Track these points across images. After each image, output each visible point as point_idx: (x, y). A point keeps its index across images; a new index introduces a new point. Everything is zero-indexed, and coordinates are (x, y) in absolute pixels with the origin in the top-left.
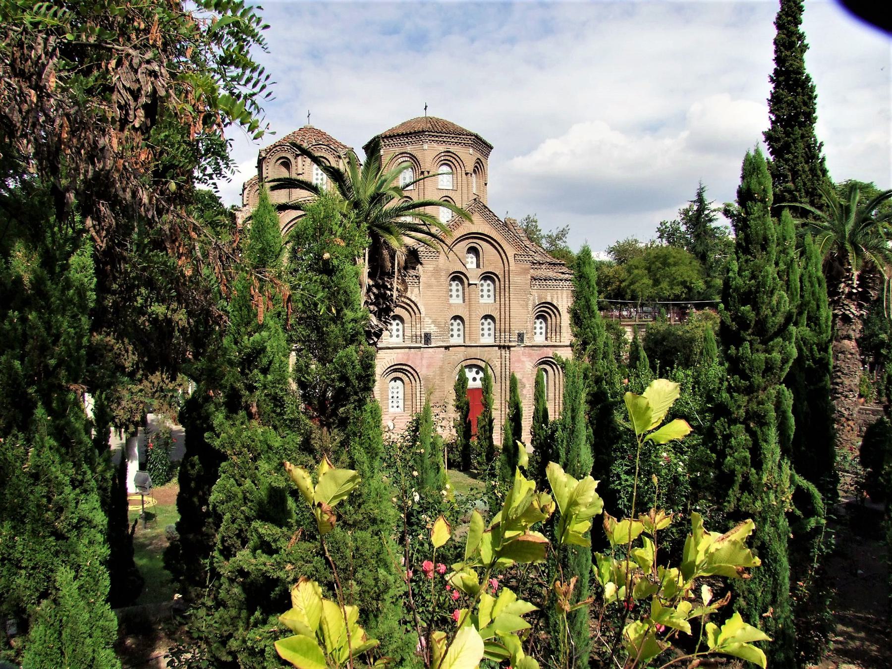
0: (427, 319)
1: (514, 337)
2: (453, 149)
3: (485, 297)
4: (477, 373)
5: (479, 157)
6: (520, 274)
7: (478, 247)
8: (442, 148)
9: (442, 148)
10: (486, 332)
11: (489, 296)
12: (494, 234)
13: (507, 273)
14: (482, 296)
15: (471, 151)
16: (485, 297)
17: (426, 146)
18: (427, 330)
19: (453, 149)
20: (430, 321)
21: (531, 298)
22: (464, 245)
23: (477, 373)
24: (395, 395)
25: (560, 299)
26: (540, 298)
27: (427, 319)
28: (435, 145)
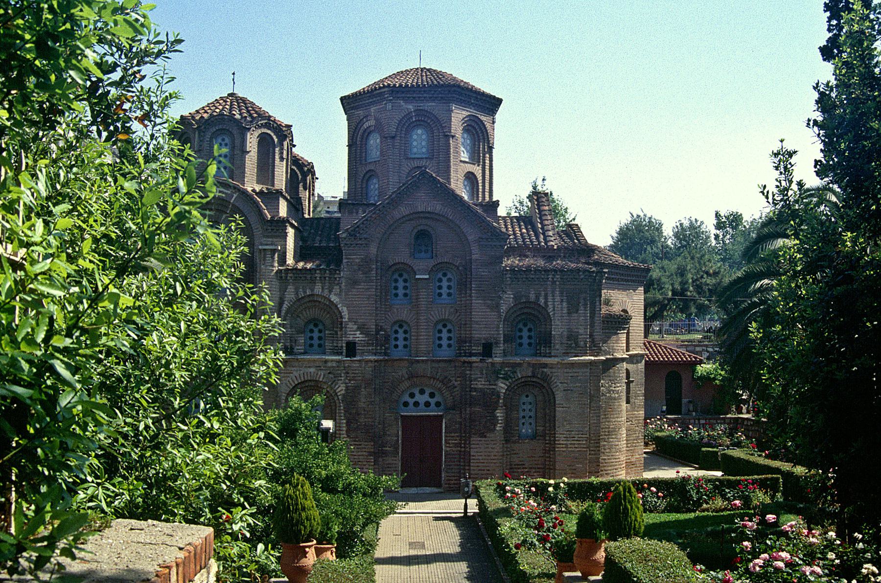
0: (350, 325)
8: (411, 107)
11: (449, 295)
14: (440, 295)
23: (432, 395)
25: (550, 298)
27: (350, 325)
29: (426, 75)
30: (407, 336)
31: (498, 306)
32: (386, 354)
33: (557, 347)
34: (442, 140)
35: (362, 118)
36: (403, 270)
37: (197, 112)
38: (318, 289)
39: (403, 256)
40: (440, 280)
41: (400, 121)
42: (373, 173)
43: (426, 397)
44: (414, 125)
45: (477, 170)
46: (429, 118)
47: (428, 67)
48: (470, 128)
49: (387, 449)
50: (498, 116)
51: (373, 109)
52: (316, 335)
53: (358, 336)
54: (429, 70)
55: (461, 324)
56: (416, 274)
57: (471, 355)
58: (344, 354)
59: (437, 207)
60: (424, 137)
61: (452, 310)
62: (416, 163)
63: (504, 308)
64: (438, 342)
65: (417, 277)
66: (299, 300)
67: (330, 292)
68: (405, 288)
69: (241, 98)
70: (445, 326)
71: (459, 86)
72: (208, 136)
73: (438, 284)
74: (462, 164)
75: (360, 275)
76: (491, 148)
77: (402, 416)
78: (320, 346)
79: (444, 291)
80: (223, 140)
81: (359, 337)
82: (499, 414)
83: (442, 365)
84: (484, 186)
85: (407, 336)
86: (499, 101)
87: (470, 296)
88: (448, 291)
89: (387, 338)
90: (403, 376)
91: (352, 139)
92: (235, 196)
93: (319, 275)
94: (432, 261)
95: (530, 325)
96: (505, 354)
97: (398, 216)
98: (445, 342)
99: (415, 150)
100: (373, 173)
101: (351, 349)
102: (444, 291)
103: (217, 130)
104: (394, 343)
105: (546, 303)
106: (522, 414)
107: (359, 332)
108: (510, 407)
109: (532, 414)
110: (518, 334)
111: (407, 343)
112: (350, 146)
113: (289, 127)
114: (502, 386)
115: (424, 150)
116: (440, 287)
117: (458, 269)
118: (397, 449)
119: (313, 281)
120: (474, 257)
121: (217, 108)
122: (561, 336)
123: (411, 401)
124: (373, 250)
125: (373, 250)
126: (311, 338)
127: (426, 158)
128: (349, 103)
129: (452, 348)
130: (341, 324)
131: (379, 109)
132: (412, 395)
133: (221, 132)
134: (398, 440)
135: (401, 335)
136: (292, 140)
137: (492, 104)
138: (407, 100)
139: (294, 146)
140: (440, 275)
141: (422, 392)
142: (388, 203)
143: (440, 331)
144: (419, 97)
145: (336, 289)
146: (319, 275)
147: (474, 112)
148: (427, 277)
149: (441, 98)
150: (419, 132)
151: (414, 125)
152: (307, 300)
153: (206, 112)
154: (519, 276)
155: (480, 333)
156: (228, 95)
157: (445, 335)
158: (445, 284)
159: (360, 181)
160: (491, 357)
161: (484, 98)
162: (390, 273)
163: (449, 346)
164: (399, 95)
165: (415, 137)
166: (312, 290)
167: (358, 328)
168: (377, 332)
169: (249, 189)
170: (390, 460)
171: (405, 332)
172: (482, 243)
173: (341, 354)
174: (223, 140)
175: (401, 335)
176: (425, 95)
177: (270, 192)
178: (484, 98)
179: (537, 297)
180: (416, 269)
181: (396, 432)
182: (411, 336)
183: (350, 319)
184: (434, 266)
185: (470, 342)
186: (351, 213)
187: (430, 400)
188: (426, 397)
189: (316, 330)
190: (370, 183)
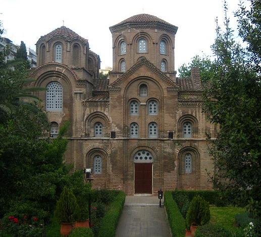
0: (113, 124)
2: (145, 30)
3: (153, 112)
4: (148, 154)
5: (165, 33)
6: (170, 99)
7: (145, 83)
8: (138, 31)
9: (138, 31)
10: (153, 132)
11: (155, 112)
12: (154, 76)
14: (151, 112)
15: (156, 31)
16: (153, 112)
18: (113, 130)
19: (145, 30)
23: (148, 154)
24: (98, 165)
25: (197, 113)
27: (113, 124)
31: (175, 116)
32: (128, 137)
33: (201, 134)
36: (134, 101)
38: (99, 110)
39: (135, 95)
40: (151, 105)
51: (123, 32)
52: (99, 129)
57: (166, 137)
59: (149, 74)
60: (144, 44)
63: (178, 118)
66: (91, 114)
67: (104, 110)
71: (159, 22)
72: (52, 45)
76: (174, 48)
77: (135, 163)
78: (100, 133)
81: (116, 129)
82: (176, 163)
83: (152, 141)
89: (128, 130)
95: (189, 125)
96: (178, 136)
98: (153, 132)
99: (141, 49)
101: (113, 135)
102: (153, 110)
104: (132, 132)
105: (196, 115)
106: (186, 163)
108: (180, 160)
109: (191, 163)
110: (184, 128)
112: (113, 48)
114: (177, 151)
115: (144, 49)
118: (133, 177)
119: (97, 106)
122: (203, 129)
123: (139, 157)
124: (122, 92)
125: (122, 92)
126: (97, 130)
128: (114, 29)
132: (139, 154)
133: (58, 43)
135: (134, 129)
137: (173, 30)
138: (136, 28)
140: (151, 103)
141: (144, 153)
143: (151, 127)
145: (107, 109)
150: (142, 42)
155: (168, 129)
157: (153, 129)
158: (153, 107)
163: (155, 133)
165: (140, 44)
170: (129, 182)
171: (136, 127)
175: (134, 129)
179: (192, 113)
181: (132, 171)
186: (114, 77)
187: (147, 156)
188: (145, 155)
189: (99, 127)
190: (122, 63)
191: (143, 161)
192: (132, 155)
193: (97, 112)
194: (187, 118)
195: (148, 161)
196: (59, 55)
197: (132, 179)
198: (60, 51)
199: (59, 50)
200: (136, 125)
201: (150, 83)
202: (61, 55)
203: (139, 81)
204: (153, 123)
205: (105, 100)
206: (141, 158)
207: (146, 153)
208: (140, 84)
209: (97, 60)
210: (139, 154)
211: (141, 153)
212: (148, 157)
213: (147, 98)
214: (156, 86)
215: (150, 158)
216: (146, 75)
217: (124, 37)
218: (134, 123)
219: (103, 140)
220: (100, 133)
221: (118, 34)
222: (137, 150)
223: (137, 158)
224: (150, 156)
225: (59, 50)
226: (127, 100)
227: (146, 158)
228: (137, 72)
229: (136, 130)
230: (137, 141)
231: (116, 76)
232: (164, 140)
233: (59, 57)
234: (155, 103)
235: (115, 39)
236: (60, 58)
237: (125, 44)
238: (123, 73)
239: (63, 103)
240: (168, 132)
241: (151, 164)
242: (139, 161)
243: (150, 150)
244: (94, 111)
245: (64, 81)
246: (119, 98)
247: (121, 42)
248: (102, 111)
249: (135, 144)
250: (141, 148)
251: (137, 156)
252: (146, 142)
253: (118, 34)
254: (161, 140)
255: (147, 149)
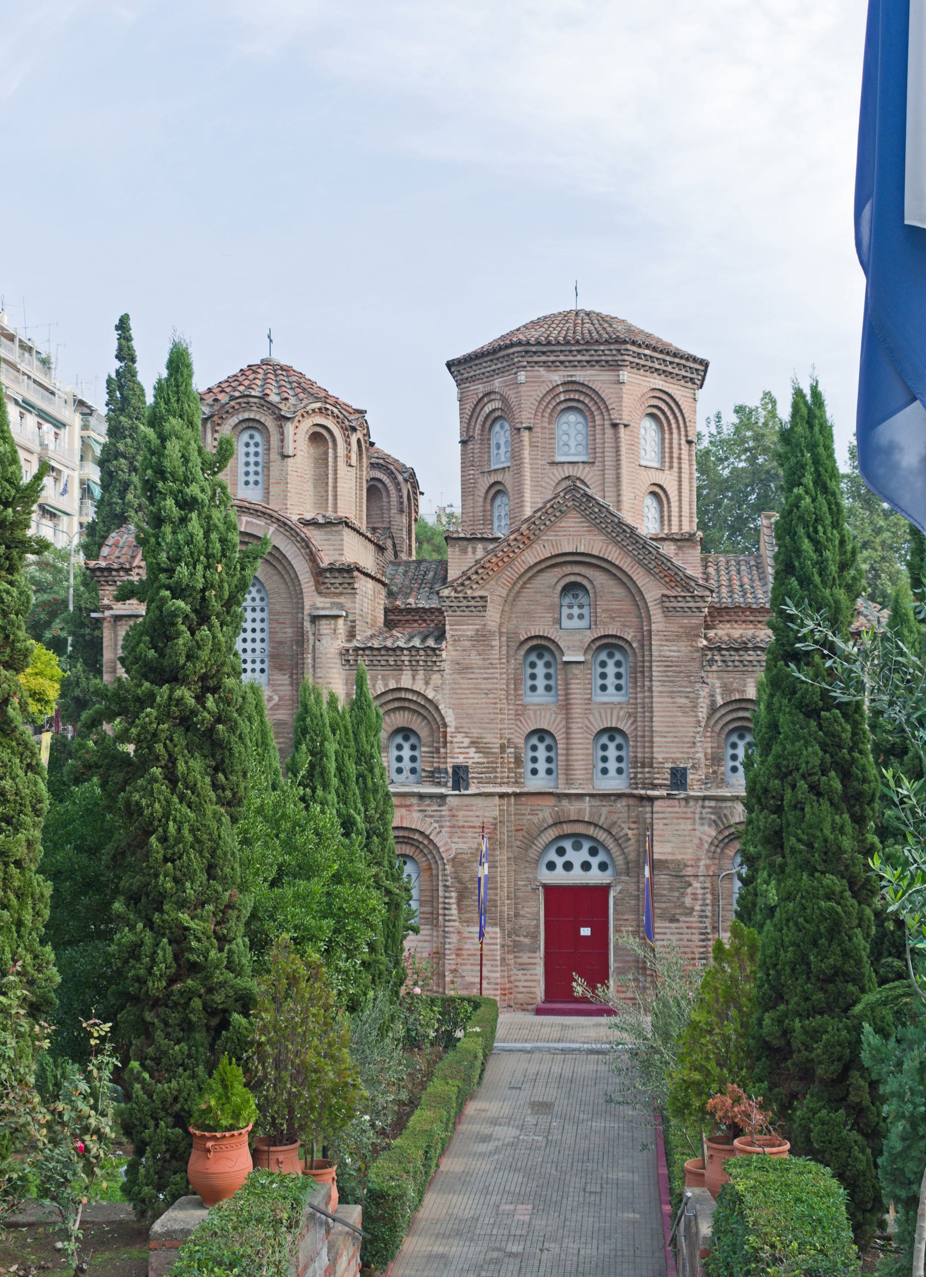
0: (459, 738)
1: (664, 777)
2: (580, 375)
3: (611, 689)
4: (593, 852)
7: (579, 579)
8: (557, 377)
9: (557, 377)
10: (612, 765)
11: (619, 688)
12: (613, 554)
13: (646, 638)
14: (604, 688)
16: (611, 689)
17: (522, 376)
18: (460, 760)
19: (580, 375)
20: (467, 741)
21: (704, 692)
22: (552, 579)
23: (593, 852)
26: (726, 689)
28: (542, 371)
29: (583, 323)
30: (552, 754)
34: (609, 432)
35: (481, 395)
37: (210, 390)
38: (406, 681)
40: (603, 664)
41: (540, 403)
42: (501, 488)
43: (584, 855)
44: (563, 406)
45: (668, 480)
46: (587, 395)
47: (588, 309)
48: (655, 411)
49: (522, 939)
50: (700, 393)
51: (497, 383)
53: (472, 755)
54: (588, 314)
55: (636, 736)
56: (563, 654)
57: (655, 787)
58: (450, 784)
61: (622, 713)
62: (568, 471)
64: (601, 765)
65: (565, 659)
67: (427, 683)
68: (548, 676)
69: (282, 369)
70: (612, 739)
73: (600, 670)
74: (643, 472)
75: (474, 659)
78: (413, 771)
79: (611, 681)
80: (252, 437)
84: (680, 507)
85: (552, 754)
86: (705, 364)
87: (650, 690)
88: (617, 682)
90: (544, 820)
91: (468, 431)
92: (272, 529)
93: (407, 658)
94: (588, 632)
97: (532, 561)
98: (612, 765)
100: (501, 488)
102: (611, 681)
103: (241, 422)
107: (474, 750)
111: (552, 766)
112: (463, 442)
113: (362, 412)
115: (580, 448)
116: (603, 676)
117: (631, 645)
118: (535, 937)
119: (398, 667)
120: (654, 627)
121: (240, 384)
123: (559, 861)
124: (493, 615)
127: (583, 463)
129: (624, 775)
130: (445, 737)
131: (505, 381)
132: (561, 852)
134: (538, 926)
135: (542, 754)
136: (368, 435)
139: (372, 444)
140: (603, 656)
141: (577, 847)
142: (515, 539)
143: (604, 748)
144: (570, 362)
146: (407, 658)
147: (658, 382)
148: (581, 659)
149: (607, 362)
151: (563, 406)
152: (390, 697)
153: (222, 391)
154: (728, 658)
156: (262, 361)
157: (612, 753)
158: (611, 670)
159: (481, 500)
160: (685, 790)
161: (677, 360)
162: (522, 652)
163: (620, 771)
164: (536, 359)
165: (565, 427)
166: (398, 682)
167: (472, 743)
168: (503, 748)
169: (295, 518)
171: (549, 748)
172: (667, 604)
173: (445, 785)
174: (252, 437)
176: (579, 358)
177: (329, 524)
178: (677, 360)
180: (562, 645)
182: (557, 754)
183: (458, 730)
184: (593, 641)
185: (651, 766)
188: (584, 855)
189: (406, 746)
190: (498, 501)
191: (577, 877)
192: (533, 853)
193: (399, 689)
194: (741, 714)
195: (595, 877)
196: (252, 469)
197: (534, 950)
198: (256, 454)
199: (252, 449)
200: (548, 741)
201: (599, 578)
202: (259, 469)
203: (559, 572)
204: (612, 732)
205: (431, 643)
206: (568, 866)
207: (586, 846)
208: (562, 583)
209: (405, 488)
210: (561, 852)
211: (567, 845)
212: (595, 862)
213: (589, 636)
214: (619, 591)
215: (603, 867)
216: (582, 549)
217: (504, 399)
218: (541, 734)
219: (421, 796)
220: (413, 771)
221: (480, 388)
222: (552, 834)
223: (551, 866)
224: (601, 857)
225: (252, 449)
226: (514, 645)
227: (586, 866)
228: (549, 536)
229: (549, 760)
230: (552, 801)
231: (474, 552)
232: (651, 799)
233: (252, 478)
234: (618, 656)
235: (469, 407)
236: (256, 483)
237: (507, 426)
238: (496, 539)
239: (272, 656)
240: (670, 765)
241: (602, 891)
242: (559, 877)
243: (602, 836)
244: (386, 685)
245: (271, 571)
246: (482, 638)
247: (493, 419)
248: (419, 686)
249: (546, 811)
250: (567, 829)
251: (552, 856)
252: (587, 803)
253: (480, 388)
254: (641, 798)
255: (591, 831)
